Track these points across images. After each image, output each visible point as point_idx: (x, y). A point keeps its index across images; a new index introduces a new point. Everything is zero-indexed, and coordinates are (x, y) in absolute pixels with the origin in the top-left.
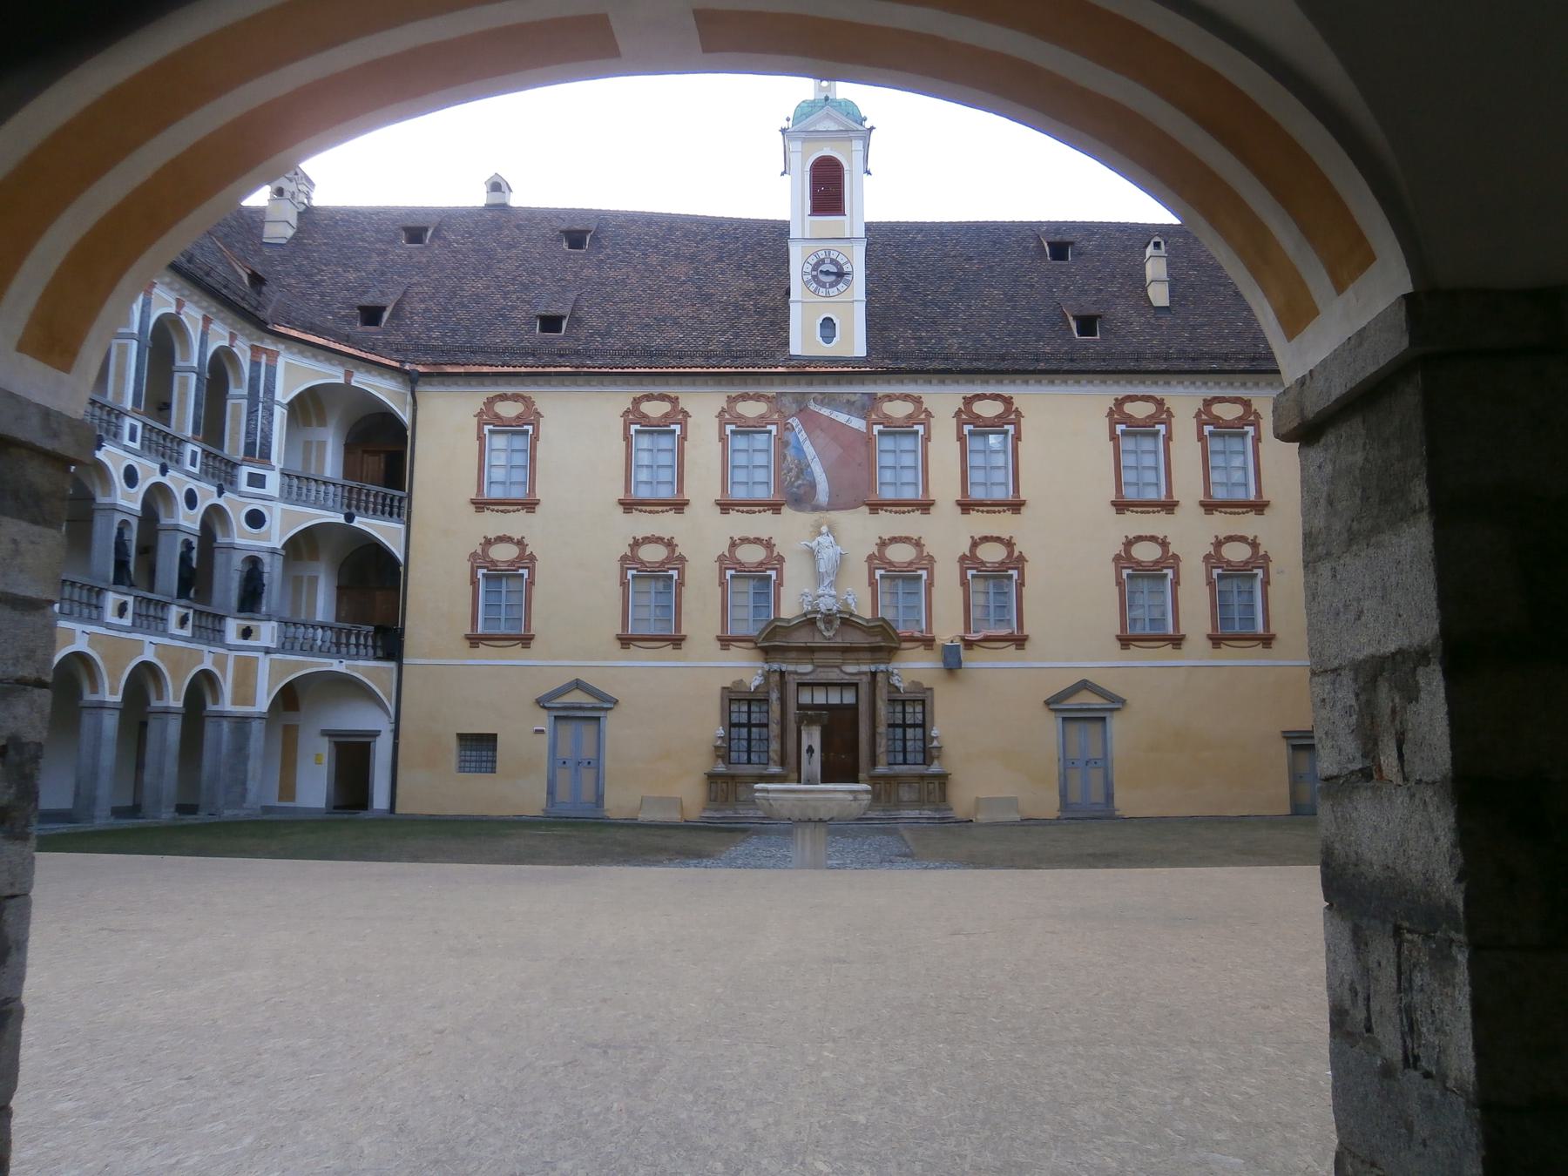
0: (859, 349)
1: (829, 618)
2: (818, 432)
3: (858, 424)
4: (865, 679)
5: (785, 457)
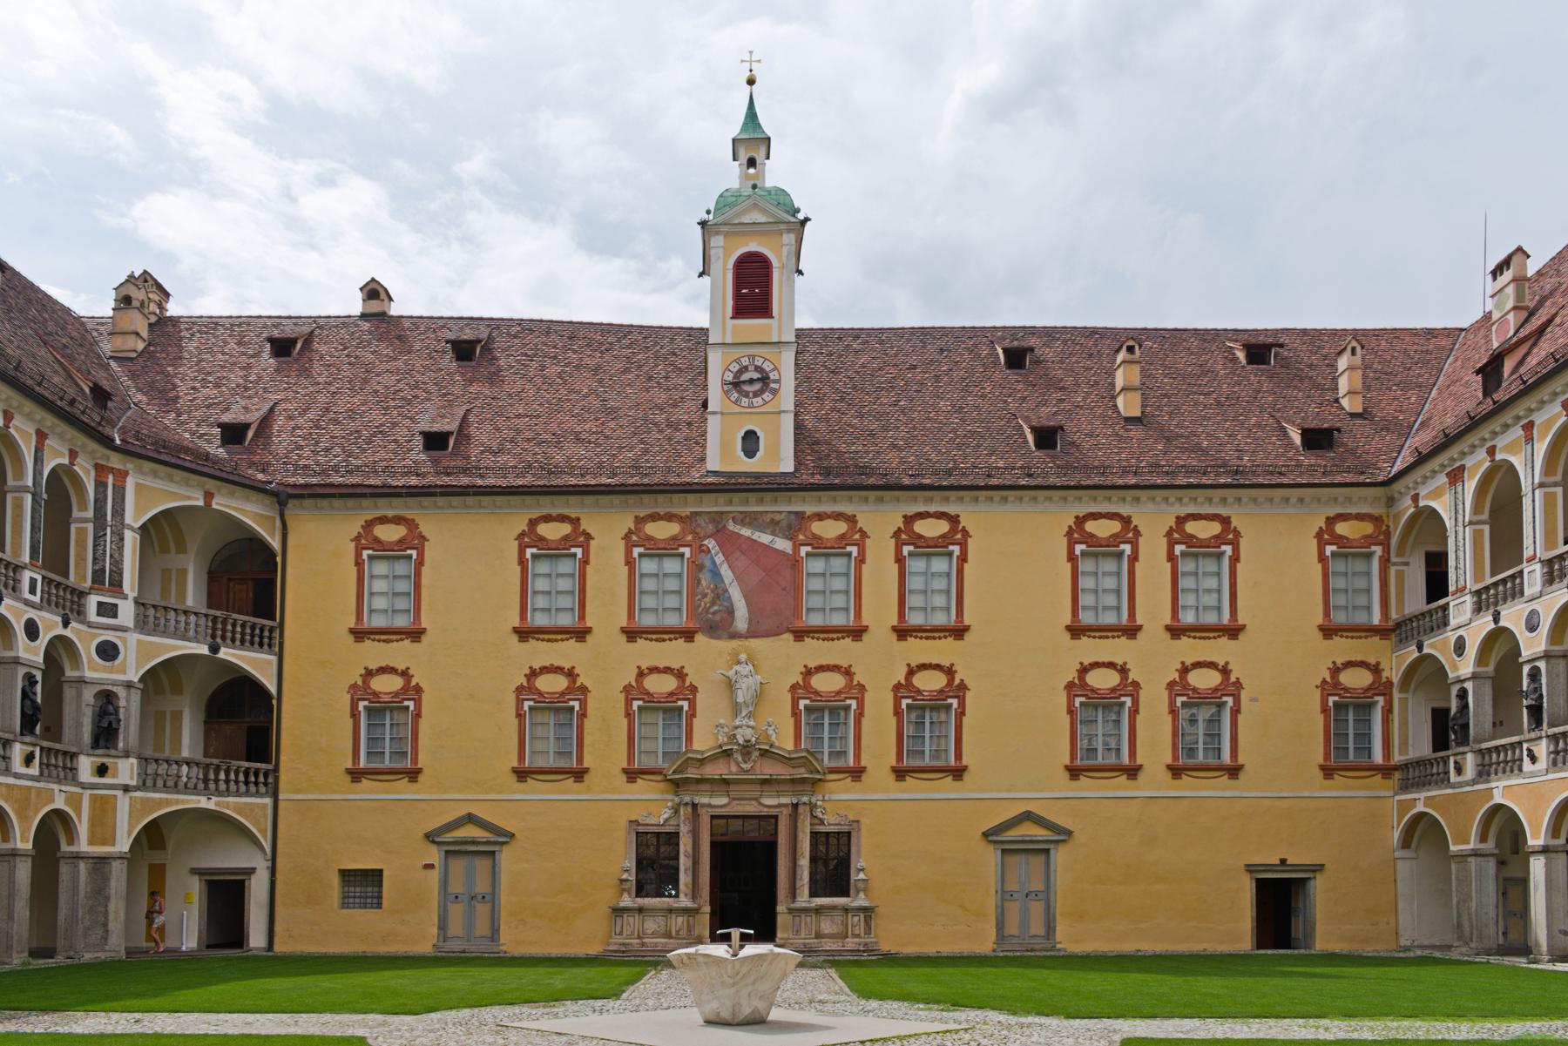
0: (788, 466)
1: (746, 749)
2: (738, 554)
3: (783, 545)
4: (786, 811)
5: (699, 582)
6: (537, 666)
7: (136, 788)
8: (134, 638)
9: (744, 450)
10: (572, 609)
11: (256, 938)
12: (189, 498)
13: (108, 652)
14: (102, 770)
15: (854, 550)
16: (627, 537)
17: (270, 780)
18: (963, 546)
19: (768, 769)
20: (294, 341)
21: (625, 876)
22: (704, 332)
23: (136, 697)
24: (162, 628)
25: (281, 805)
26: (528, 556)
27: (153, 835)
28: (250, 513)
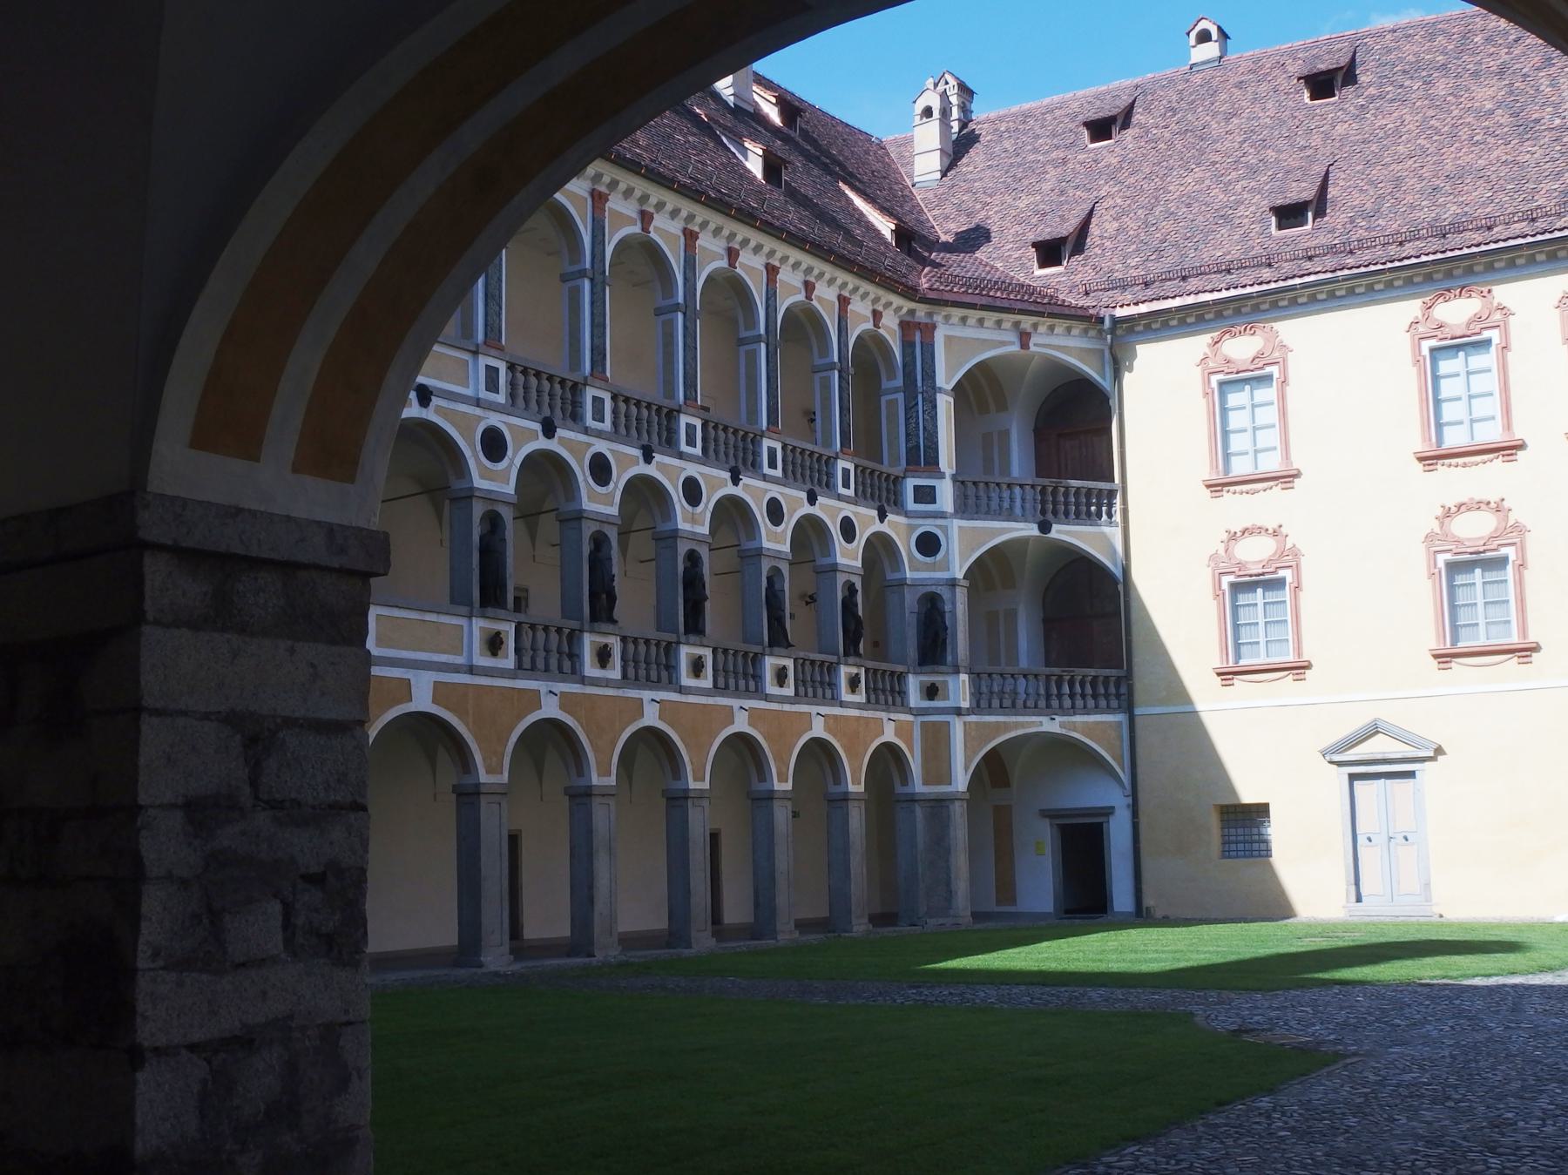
6: (1451, 503)
7: (970, 712)
8: (957, 523)
11: (1122, 898)
12: (1004, 343)
13: (929, 544)
14: (931, 692)
17: (1123, 690)
23: (961, 596)
24: (984, 508)
25: (1138, 721)
27: (994, 769)
28: (1063, 346)
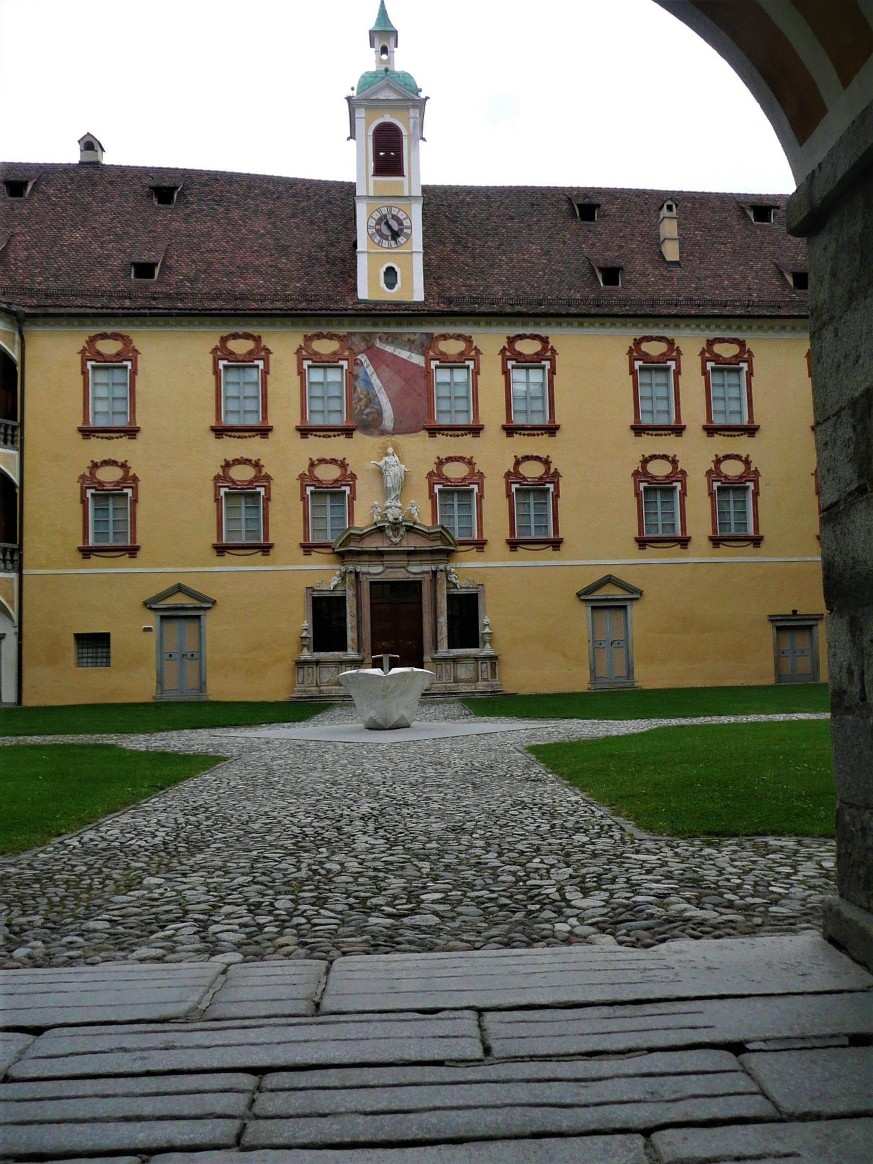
0: (419, 295)
1: (395, 526)
2: (384, 367)
3: (418, 359)
4: (428, 577)
5: (355, 389)
6: (230, 459)
9: (385, 282)
10: (257, 412)
15: (471, 364)
16: (298, 352)
17: (16, 557)
18: (552, 360)
19: (413, 543)
20: (25, 184)
21: (304, 634)
22: (352, 186)
25: (25, 579)
26: (221, 367)
